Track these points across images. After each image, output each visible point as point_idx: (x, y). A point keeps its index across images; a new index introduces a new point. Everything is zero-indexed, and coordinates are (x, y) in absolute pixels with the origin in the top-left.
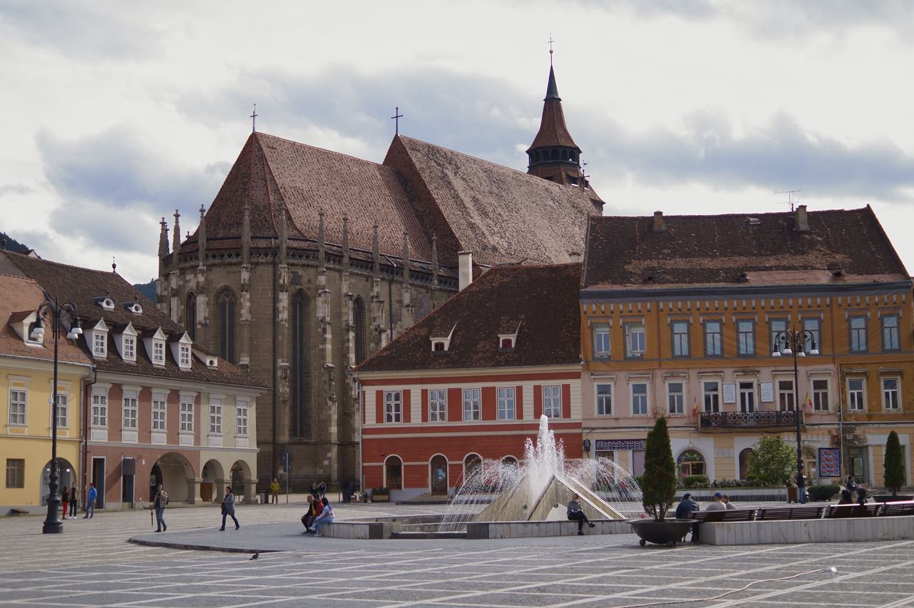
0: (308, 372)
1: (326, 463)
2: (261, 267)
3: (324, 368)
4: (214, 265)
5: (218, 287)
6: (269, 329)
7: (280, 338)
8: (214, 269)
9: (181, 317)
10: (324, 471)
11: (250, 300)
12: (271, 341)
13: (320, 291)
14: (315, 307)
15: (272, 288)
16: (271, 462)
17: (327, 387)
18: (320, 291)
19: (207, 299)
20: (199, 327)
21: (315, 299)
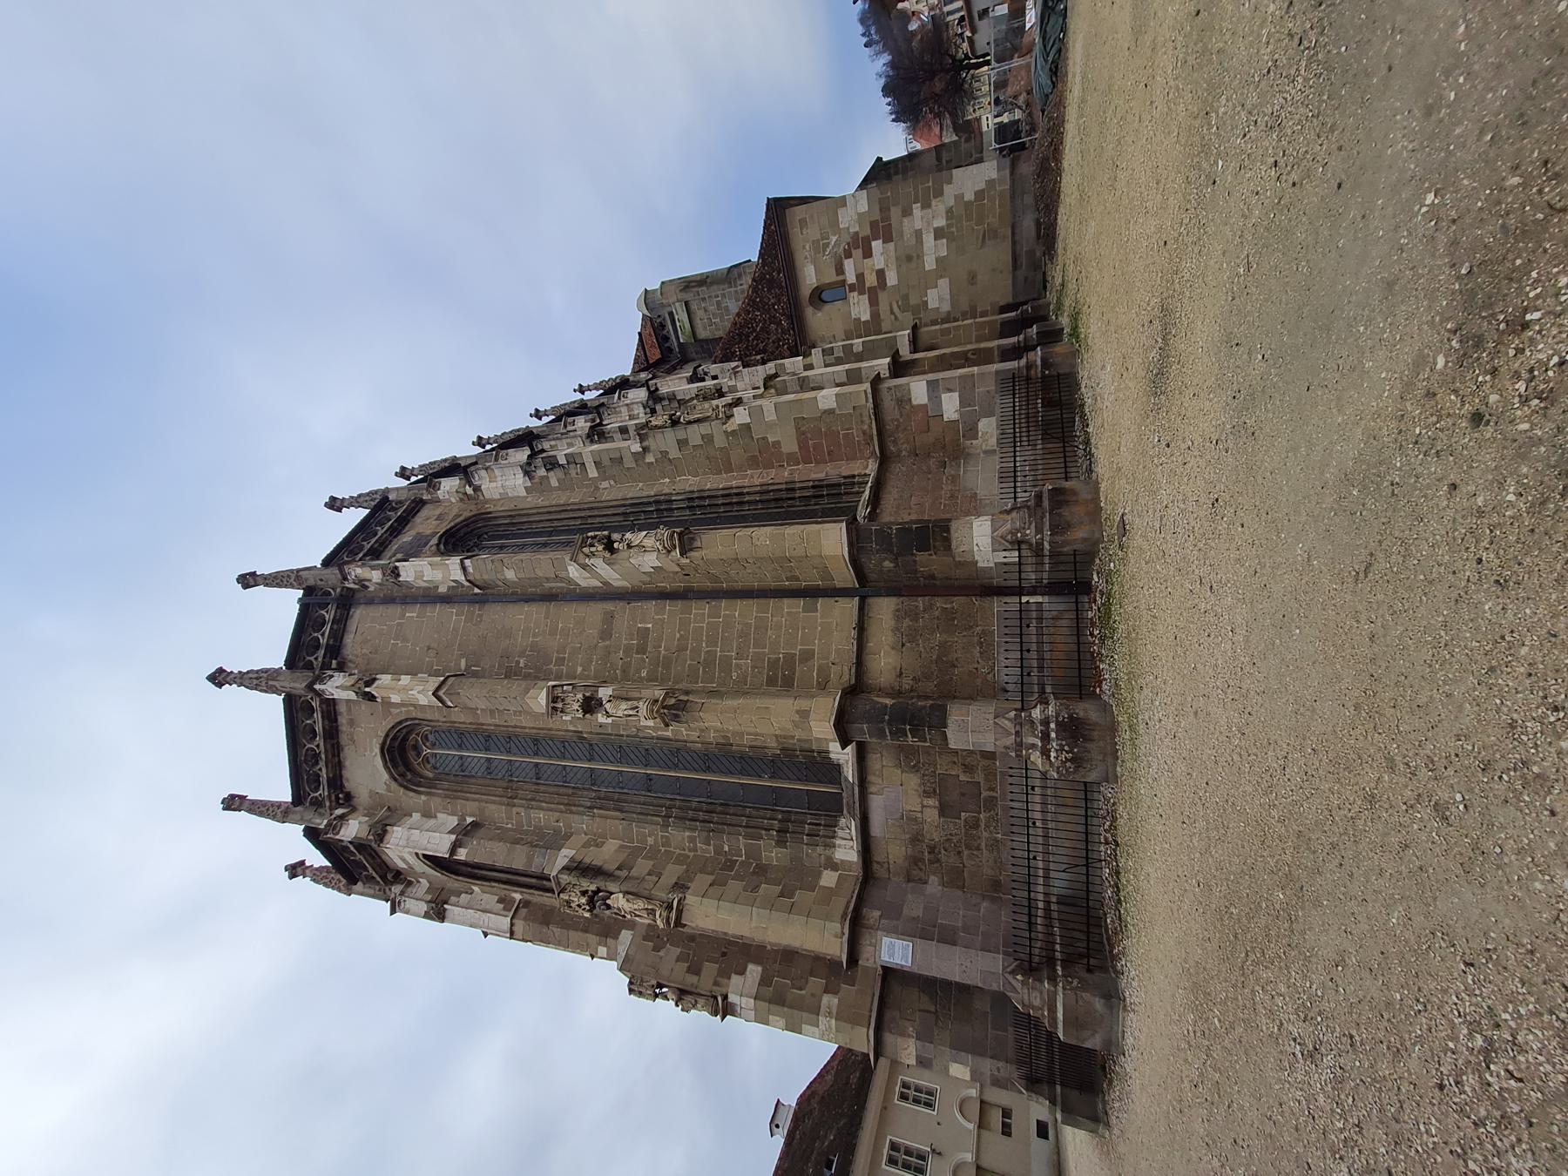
0: (657, 502)
1: (950, 406)
2: (349, 639)
3: (646, 450)
4: (336, 783)
5: (386, 776)
6: (496, 615)
7: (510, 575)
8: (348, 786)
9: (500, 901)
10: (990, 414)
11: (397, 673)
12: (526, 608)
13: (469, 490)
14: (504, 498)
15: (394, 610)
16: (940, 603)
17: (695, 434)
18: (469, 490)
19: (416, 816)
20: (462, 854)
21: (487, 501)
